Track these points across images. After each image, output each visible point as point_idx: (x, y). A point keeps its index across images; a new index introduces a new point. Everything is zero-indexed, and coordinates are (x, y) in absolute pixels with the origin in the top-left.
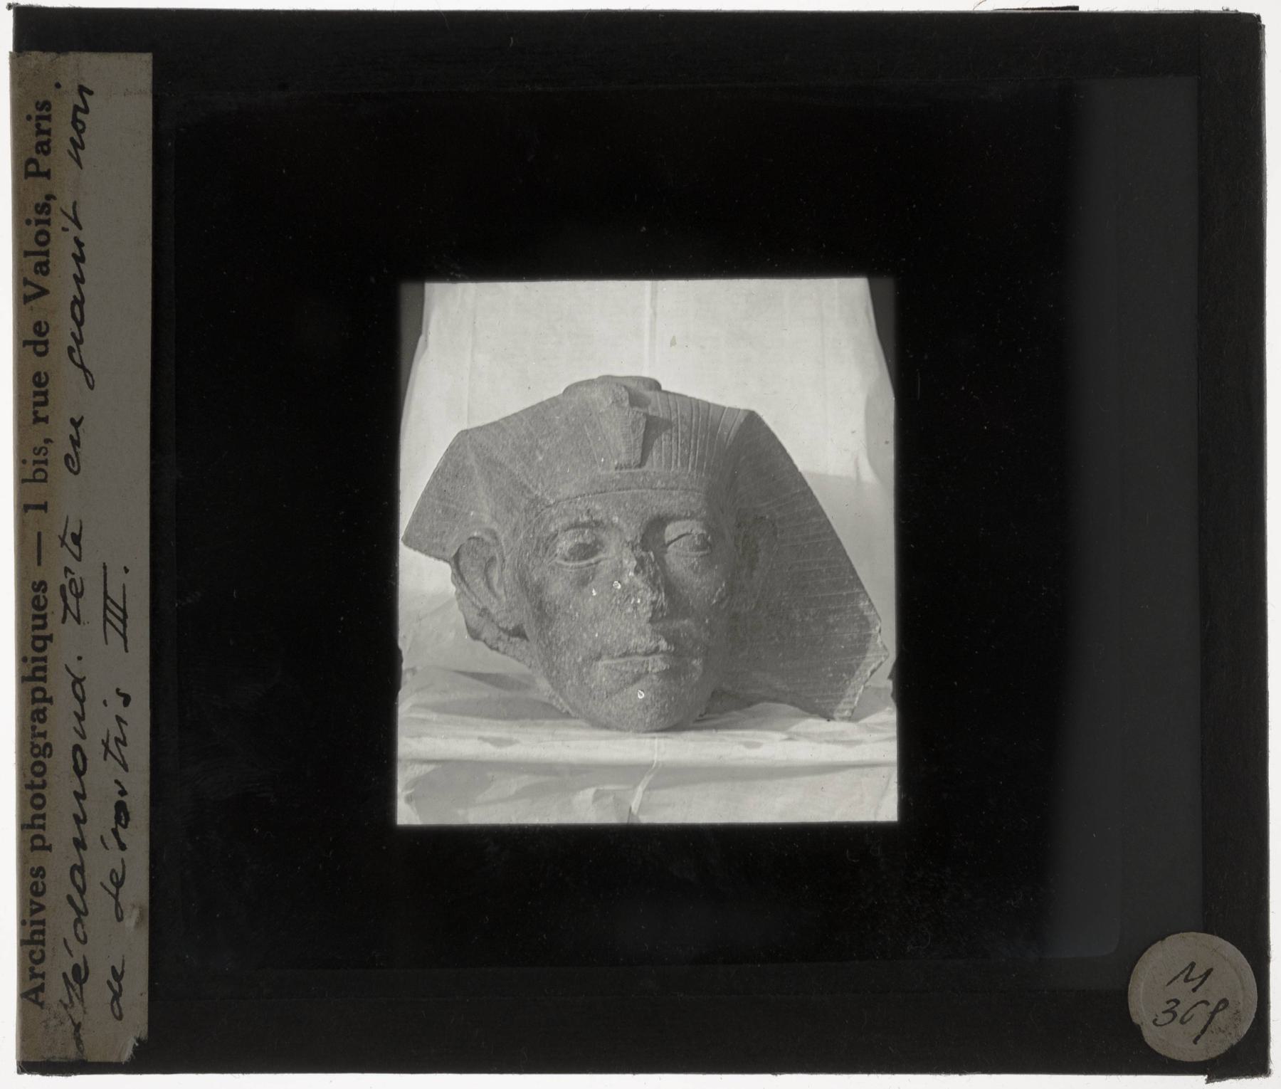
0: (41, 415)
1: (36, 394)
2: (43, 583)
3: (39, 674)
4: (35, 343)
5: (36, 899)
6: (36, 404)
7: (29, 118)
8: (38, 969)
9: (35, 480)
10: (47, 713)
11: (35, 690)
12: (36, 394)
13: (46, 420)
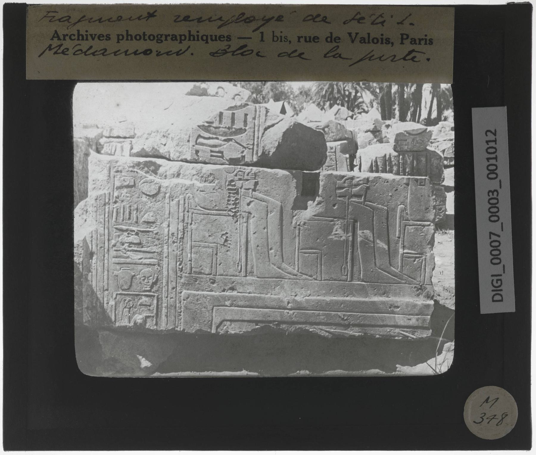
4: (331, 37)
5: (97, 37)
6: (306, 37)
7: (426, 36)
8: (67, 38)
9: (274, 36)
10: (175, 41)
11: (184, 35)
12: (310, 37)
13: (299, 41)
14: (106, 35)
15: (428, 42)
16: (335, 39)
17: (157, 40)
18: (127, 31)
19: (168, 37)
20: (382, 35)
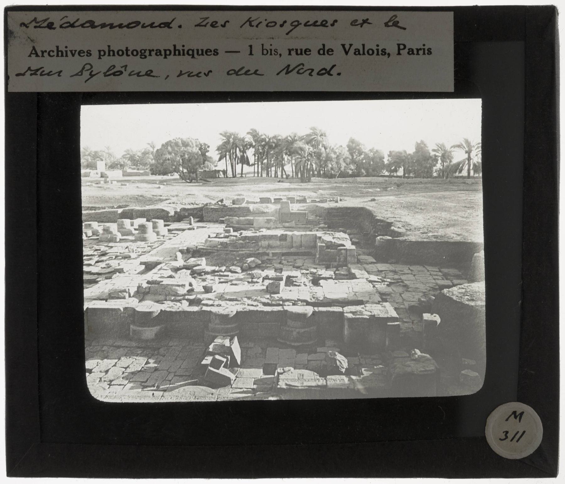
0: (292, 52)
1: (301, 50)
2: (218, 54)
3: (177, 52)
4: (324, 49)
5: (77, 52)
6: (297, 50)
7: (424, 45)
8: (46, 54)
9: (263, 50)
11: (170, 51)
13: (290, 54)
15: (426, 52)
16: (328, 51)
17: (141, 55)
18: (109, 46)
19: (152, 52)
20: (378, 46)
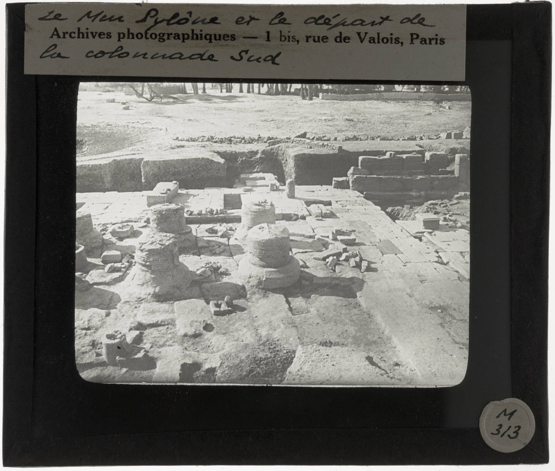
0: (309, 39)
1: (319, 37)
3: (195, 36)
5: (97, 35)
6: (314, 37)
7: (436, 35)
8: (67, 36)
9: (281, 36)
11: (188, 35)
13: (307, 41)
14: (107, 34)
16: (345, 38)
17: (160, 39)
18: (129, 30)
20: (391, 34)
